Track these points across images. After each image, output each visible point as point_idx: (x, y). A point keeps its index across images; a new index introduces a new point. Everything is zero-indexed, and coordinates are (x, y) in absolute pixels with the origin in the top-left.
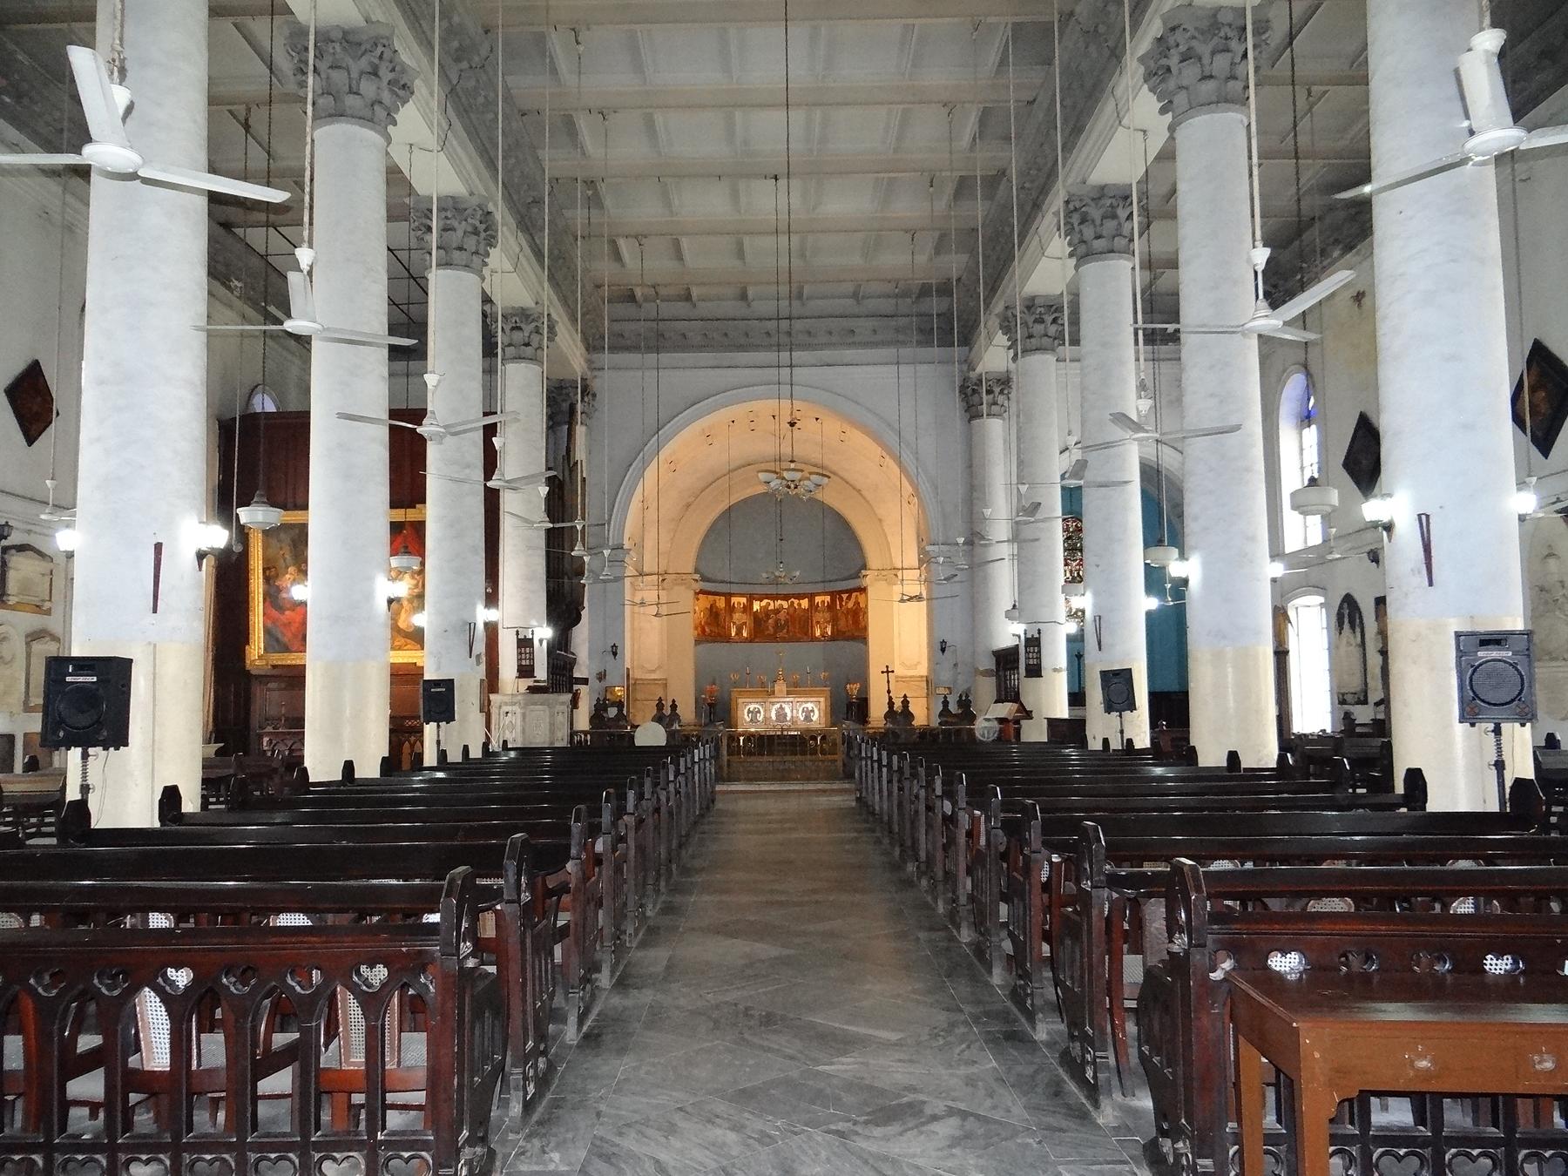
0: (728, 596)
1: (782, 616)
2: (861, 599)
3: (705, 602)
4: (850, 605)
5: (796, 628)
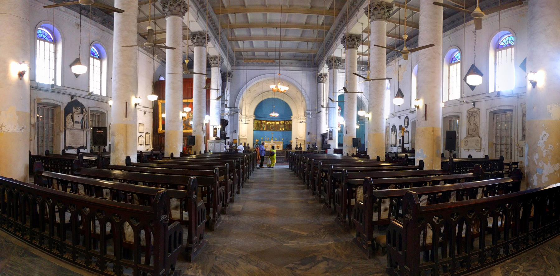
3: (256, 122)
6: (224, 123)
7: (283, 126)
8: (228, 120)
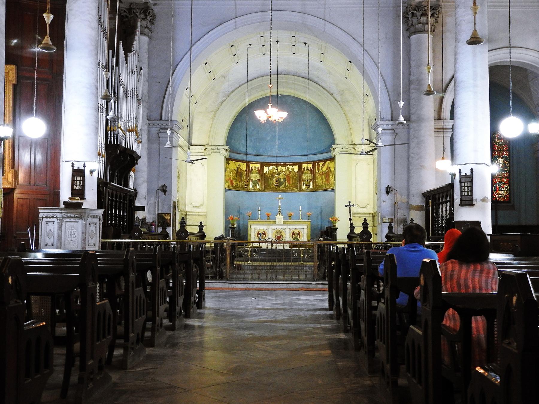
0: (248, 163)
1: (282, 176)
2: (331, 165)
3: (233, 165)
4: (324, 169)
5: (292, 184)
6: (119, 159)
7: (310, 176)
8: (137, 149)
